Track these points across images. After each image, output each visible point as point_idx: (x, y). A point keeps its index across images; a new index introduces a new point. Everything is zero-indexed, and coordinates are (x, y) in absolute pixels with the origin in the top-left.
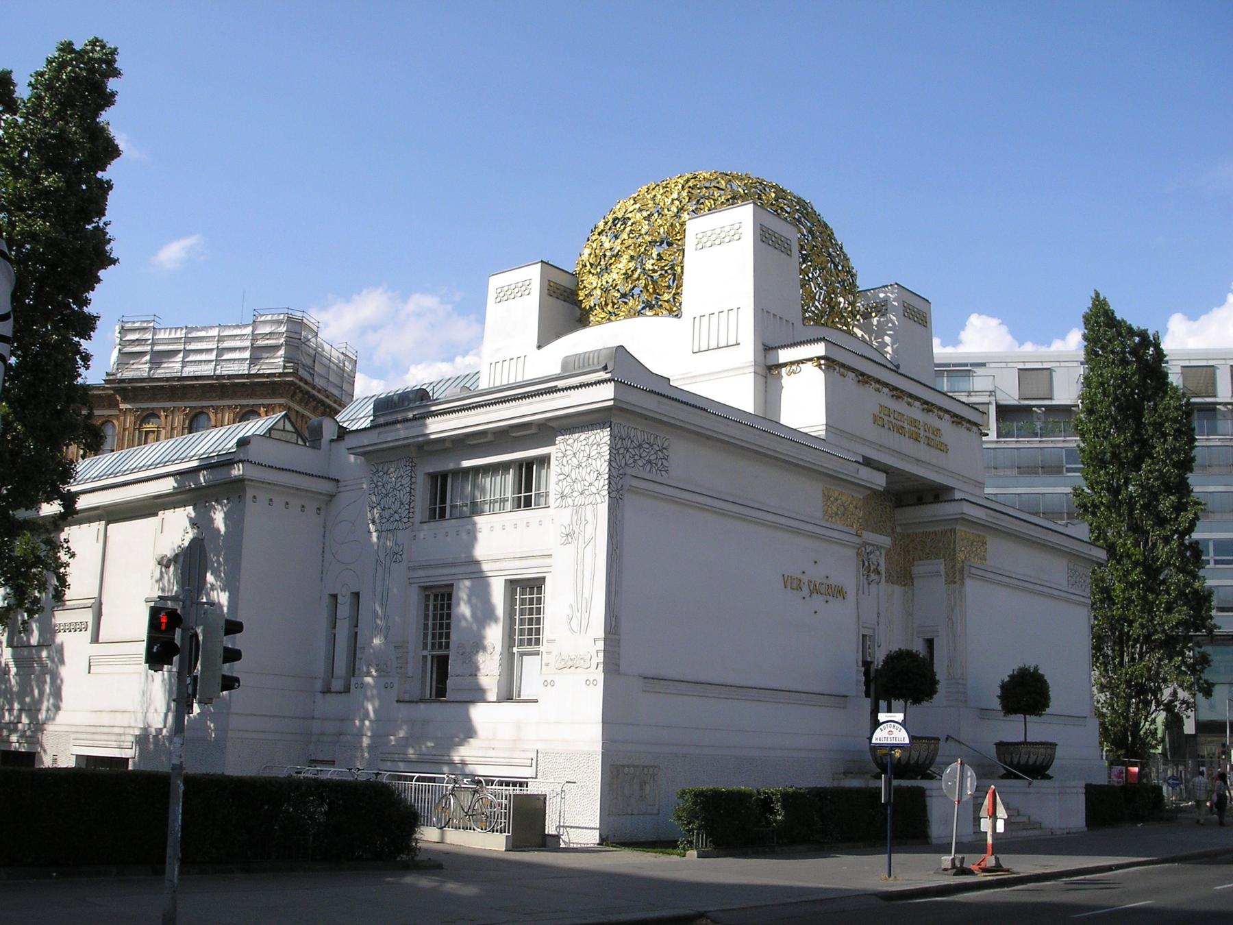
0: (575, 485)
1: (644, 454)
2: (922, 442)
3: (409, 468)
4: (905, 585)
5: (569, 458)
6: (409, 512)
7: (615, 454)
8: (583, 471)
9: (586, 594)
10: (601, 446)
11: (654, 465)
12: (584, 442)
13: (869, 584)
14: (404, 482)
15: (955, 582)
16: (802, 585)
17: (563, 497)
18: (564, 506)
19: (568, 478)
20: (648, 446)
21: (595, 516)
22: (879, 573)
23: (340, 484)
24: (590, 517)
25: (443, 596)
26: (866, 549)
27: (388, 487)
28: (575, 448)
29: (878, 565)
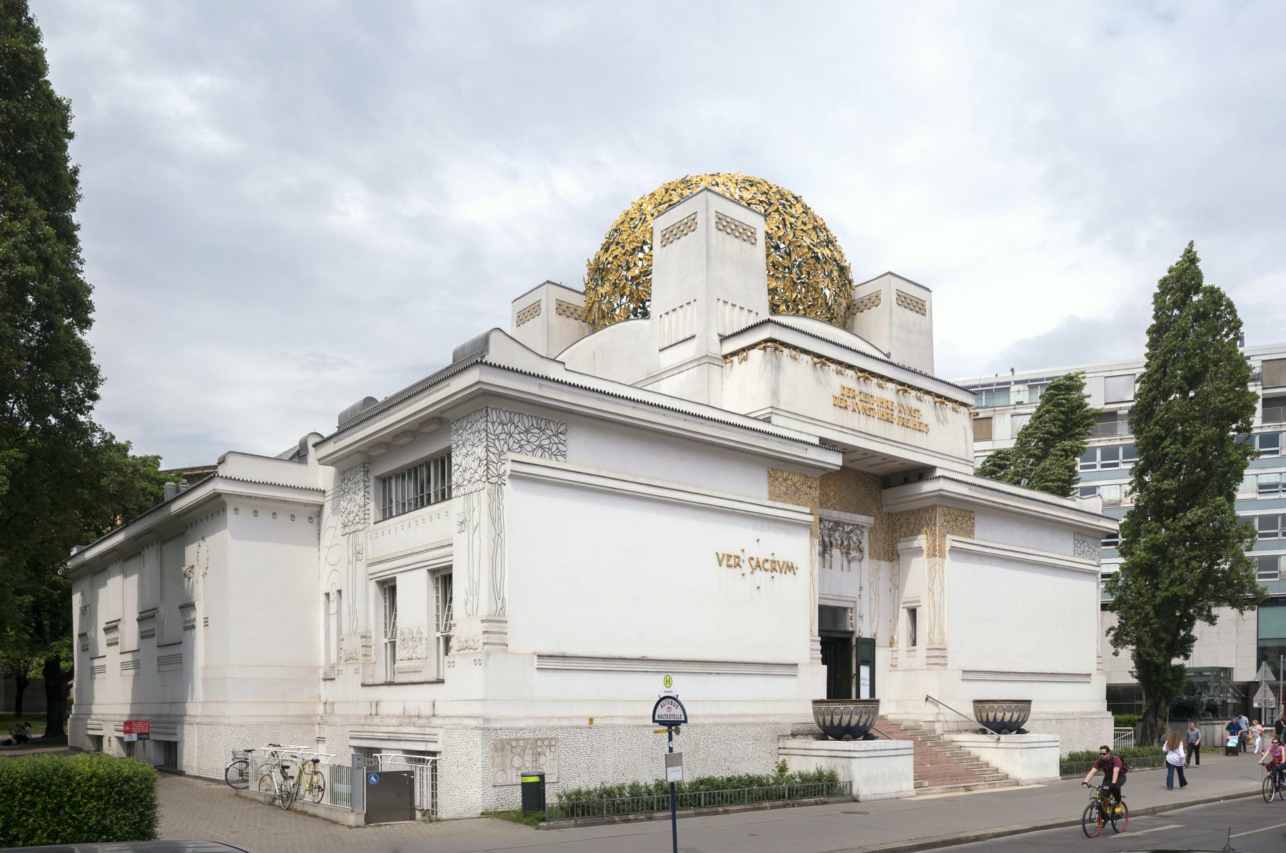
1: (533, 439)
2: (895, 423)
4: (892, 561)
6: (365, 514)
7: (494, 440)
8: (470, 459)
11: (547, 450)
12: (470, 431)
13: (849, 562)
14: (360, 487)
15: (935, 556)
16: (741, 564)
17: (458, 486)
20: (539, 432)
22: (861, 551)
26: (843, 529)
29: (860, 543)
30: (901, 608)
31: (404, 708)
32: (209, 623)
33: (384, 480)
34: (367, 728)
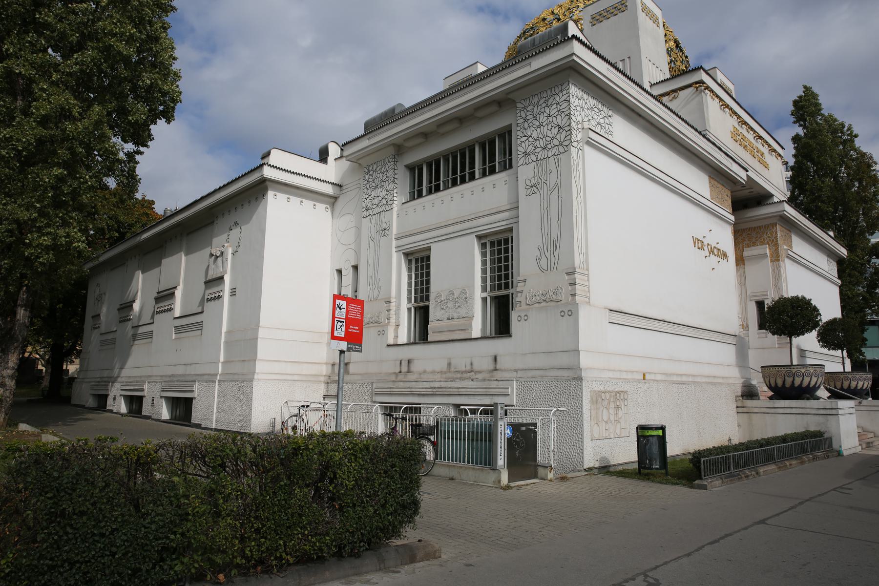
0: (538, 142)
3: (392, 163)
5: (529, 121)
9: (554, 235)
10: (560, 104)
12: (544, 105)
14: (389, 175)
17: (526, 154)
18: (528, 163)
19: (530, 139)
21: (558, 165)
23: (344, 188)
24: (553, 167)
25: (422, 259)
27: (377, 181)
28: (535, 113)
30: (748, 300)
31: (449, 364)
32: (237, 293)
33: (411, 168)
34: (401, 384)
